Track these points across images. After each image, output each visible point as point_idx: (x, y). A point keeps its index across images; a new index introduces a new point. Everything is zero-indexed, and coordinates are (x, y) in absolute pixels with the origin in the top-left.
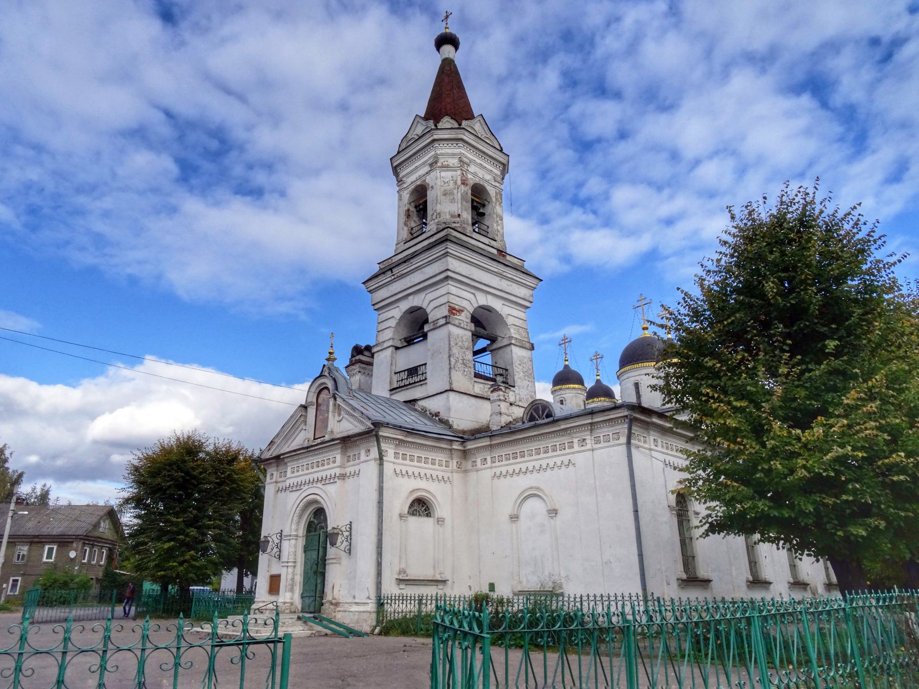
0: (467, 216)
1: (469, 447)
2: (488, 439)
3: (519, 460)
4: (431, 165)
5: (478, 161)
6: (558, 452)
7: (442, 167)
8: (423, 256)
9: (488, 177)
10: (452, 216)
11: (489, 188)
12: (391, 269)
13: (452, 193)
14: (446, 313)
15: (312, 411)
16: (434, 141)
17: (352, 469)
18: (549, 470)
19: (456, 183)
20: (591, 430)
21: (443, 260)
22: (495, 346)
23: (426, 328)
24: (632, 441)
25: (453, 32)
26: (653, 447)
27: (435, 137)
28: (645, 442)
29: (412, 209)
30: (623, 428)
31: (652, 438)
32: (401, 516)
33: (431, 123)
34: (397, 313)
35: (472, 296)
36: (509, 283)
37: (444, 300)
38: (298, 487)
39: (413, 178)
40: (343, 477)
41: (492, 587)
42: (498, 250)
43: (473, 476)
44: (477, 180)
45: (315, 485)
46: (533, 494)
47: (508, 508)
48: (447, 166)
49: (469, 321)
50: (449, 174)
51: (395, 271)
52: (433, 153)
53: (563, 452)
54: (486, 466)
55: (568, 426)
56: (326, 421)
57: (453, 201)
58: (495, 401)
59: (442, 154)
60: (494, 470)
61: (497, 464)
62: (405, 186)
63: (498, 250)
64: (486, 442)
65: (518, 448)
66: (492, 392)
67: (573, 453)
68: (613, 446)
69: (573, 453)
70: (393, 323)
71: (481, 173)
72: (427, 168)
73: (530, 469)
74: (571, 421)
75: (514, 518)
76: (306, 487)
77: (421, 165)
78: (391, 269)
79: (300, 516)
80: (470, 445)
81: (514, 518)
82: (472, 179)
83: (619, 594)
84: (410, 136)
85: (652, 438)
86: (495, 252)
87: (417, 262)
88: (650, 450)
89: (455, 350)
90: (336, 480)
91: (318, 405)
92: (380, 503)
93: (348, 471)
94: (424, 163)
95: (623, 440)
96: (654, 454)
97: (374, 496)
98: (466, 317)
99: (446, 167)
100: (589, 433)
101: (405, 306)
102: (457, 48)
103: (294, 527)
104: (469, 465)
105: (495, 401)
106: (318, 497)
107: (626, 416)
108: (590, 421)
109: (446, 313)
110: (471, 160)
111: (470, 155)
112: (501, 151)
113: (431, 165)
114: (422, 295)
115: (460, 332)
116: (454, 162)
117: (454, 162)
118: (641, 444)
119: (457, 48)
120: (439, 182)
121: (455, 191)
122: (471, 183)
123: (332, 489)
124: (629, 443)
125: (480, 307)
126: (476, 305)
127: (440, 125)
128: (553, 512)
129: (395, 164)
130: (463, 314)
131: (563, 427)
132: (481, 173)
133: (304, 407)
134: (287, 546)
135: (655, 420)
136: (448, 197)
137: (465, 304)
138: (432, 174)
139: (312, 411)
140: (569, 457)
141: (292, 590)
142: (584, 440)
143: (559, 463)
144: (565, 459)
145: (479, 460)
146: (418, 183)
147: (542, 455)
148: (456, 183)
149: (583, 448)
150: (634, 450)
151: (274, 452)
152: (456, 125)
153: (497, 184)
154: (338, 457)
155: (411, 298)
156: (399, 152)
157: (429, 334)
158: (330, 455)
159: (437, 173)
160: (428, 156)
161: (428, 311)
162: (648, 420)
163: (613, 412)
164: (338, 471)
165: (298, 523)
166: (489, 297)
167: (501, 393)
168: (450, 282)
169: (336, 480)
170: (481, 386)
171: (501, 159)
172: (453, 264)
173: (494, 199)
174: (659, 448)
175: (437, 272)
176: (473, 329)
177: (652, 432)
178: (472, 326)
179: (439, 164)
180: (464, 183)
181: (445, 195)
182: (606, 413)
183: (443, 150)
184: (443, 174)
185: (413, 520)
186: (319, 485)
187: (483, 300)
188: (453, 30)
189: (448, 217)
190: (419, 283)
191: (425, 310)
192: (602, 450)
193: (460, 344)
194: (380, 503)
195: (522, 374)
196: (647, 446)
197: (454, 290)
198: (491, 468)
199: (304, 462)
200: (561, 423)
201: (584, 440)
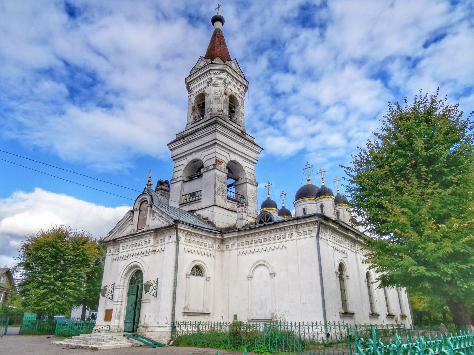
0: (226, 111)
1: (225, 237)
2: (237, 233)
3: (254, 245)
4: (208, 83)
5: (233, 83)
6: (277, 241)
7: (214, 84)
8: (202, 131)
9: (238, 92)
10: (219, 111)
11: (238, 98)
12: (183, 138)
13: (219, 99)
14: (214, 163)
15: (136, 213)
16: (210, 70)
17: (160, 248)
18: (271, 251)
19: (221, 93)
20: (296, 229)
21: (214, 134)
22: (237, 183)
23: (202, 171)
24: (320, 235)
25: (222, 15)
26: (328, 239)
27: (211, 68)
28: (325, 236)
29: (196, 106)
30: (315, 228)
31: (328, 234)
32: (187, 276)
33: (209, 61)
34: (185, 162)
35: (228, 155)
36: (247, 149)
37: (213, 155)
39: (197, 89)
40: (154, 252)
41: (235, 317)
42: (242, 131)
43: (226, 253)
44: (232, 93)
45: (136, 256)
46: (262, 264)
47: (247, 272)
48: (217, 84)
49: (225, 168)
50: (218, 88)
51: (186, 139)
52: (210, 76)
53: (280, 241)
54: (234, 248)
55: (283, 226)
56: (145, 219)
57: (219, 103)
58: (240, 212)
59: (214, 77)
60: (239, 250)
61: (241, 247)
62: (193, 93)
63: (242, 131)
64: (235, 234)
65: (253, 238)
66: (238, 207)
67: (286, 241)
68: (308, 238)
69: (286, 241)
70: (183, 168)
71: (234, 90)
72: (206, 85)
73: (260, 250)
74: (285, 223)
75: (250, 277)
76: (131, 257)
77: (202, 83)
78: (183, 138)
79: (127, 275)
80: (226, 236)
81: (250, 277)
82: (229, 93)
83: (314, 322)
84: (197, 67)
85: (328, 234)
86: (240, 132)
87: (198, 135)
88: (327, 240)
89: (218, 183)
90: (150, 253)
91: (140, 211)
92: (176, 267)
93: (157, 248)
94: (204, 82)
95: (315, 234)
96: (329, 243)
97: (173, 263)
98: (224, 166)
99: (217, 85)
100: (295, 230)
101: (190, 158)
102: (223, 23)
103: (122, 281)
104: (224, 247)
105: (240, 212)
106: (138, 264)
107: (317, 221)
108: (296, 223)
109: (214, 163)
110: (230, 82)
111: (229, 79)
112: (245, 79)
113: (208, 83)
114: (201, 153)
115: (221, 174)
116: (221, 82)
117: (221, 82)
118: (323, 237)
119: (223, 23)
120: (212, 92)
121: (221, 98)
122: (229, 94)
123: (146, 259)
124: (318, 236)
125: (231, 161)
126: (229, 160)
127: (214, 62)
128: (273, 275)
129: (188, 82)
130: (223, 164)
131: (280, 227)
132: (234, 90)
135: (331, 224)
137: (224, 158)
138: (209, 88)
139: (136, 213)
140: (283, 243)
142: (292, 234)
143: (277, 247)
144: (281, 245)
145: (230, 245)
146: (200, 92)
147: (267, 242)
148: (221, 93)
149: (291, 239)
150: (320, 240)
151: (112, 237)
152: (223, 63)
153: (242, 97)
154: (152, 240)
155: (194, 154)
156: (190, 75)
158: (147, 239)
160: (207, 78)
161: (203, 161)
162: (327, 224)
163: (310, 218)
164: (151, 248)
165: (125, 279)
166: (236, 156)
167: (243, 208)
168: (217, 146)
169: (150, 253)
170: (231, 204)
171: (244, 83)
172: (219, 136)
173: (240, 104)
174: (331, 240)
175: (210, 140)
176: (228, 172)
177: (328, 231)
178: (227, 171)
179: (213, 83)
180: (226, 94)
181: (215, 99)
182: (306, 219)
183: (215, 75)
184: (215, 88)
185: (194, 278)
186: (139, 256)
187: (233, 157)
188: (221, 14)
189: (216, 111)
191: (202, 161)
192: (302, 240)
193: (221, 180)
194: (176, 267)
195: (251, 199)
196: (325, 238)
197: (218, 151)
198: (238, 249)
199: (131, 243)
200: (280, 224)
201: (292, 234)
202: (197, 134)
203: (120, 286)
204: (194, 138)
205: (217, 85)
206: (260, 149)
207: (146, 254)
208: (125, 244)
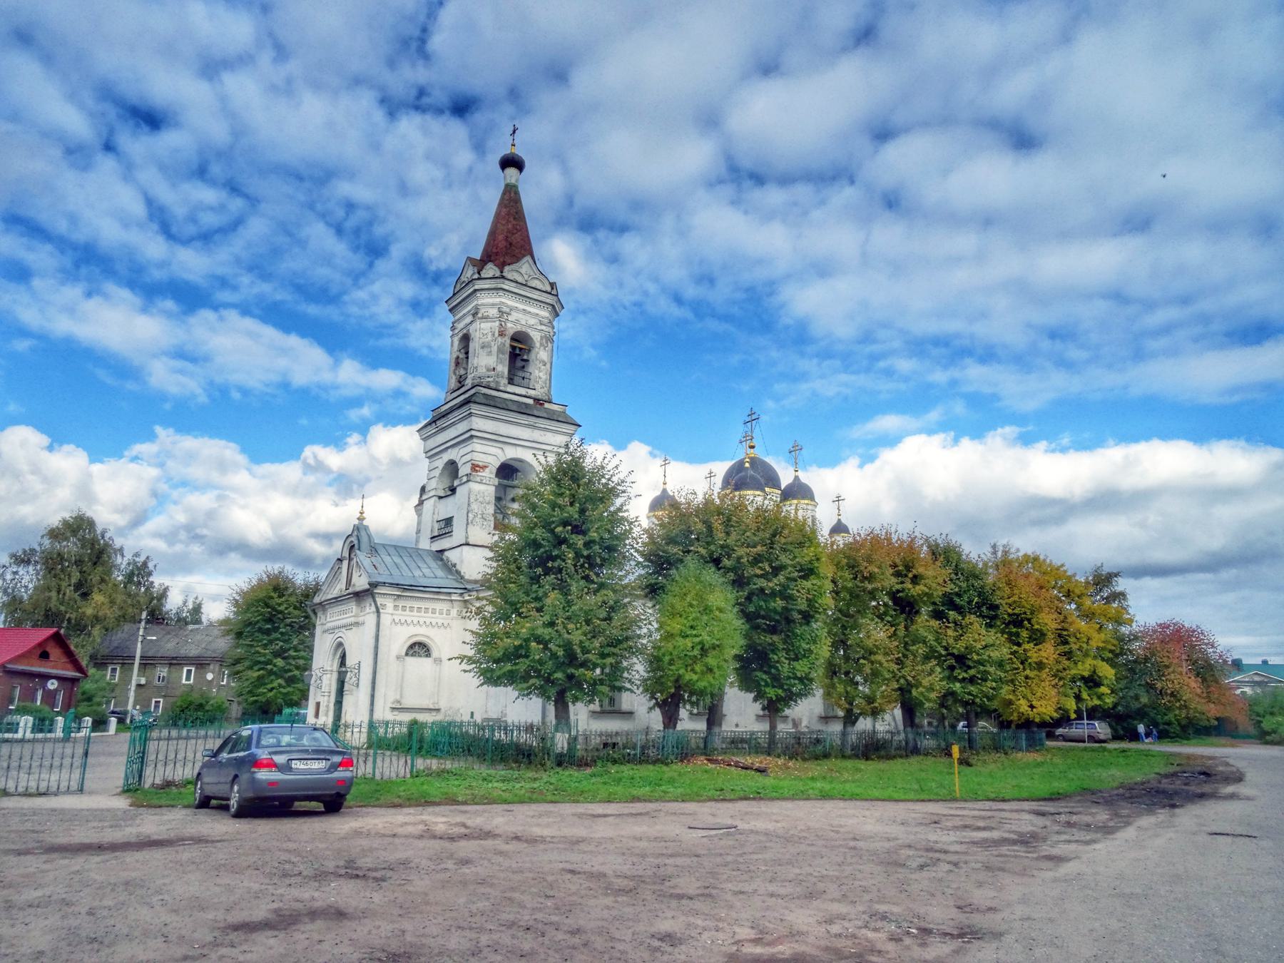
0: (503, 369)
5: (521, 306)
7: (482, 318)
8: (456, 413)
9: (532, 321)
14: (469, 471)
15: (345, 563)
16: (475, 291)
40: (357, 624)
42: (535, 399)
44: (519, 328)
50: (489, 325)
57: (490, 353)
63: (535, 399)
71: (523, 319)
79: (335, 654)
82: (511, 328)
89: (474, 506)
91: (350, 559)
92: (376, 648)
97: (372, 641)
99: (485, 318)
109: (469, 471)
111: (510, 302)
114: (456, 449)
117: (493, 312)
122: (510, 332)
133: (340, 560)
134: (326, 679)
136: (486, 350)
137: (489, 459)
139: (345, 563)
141: (327, 715)
152: (498, 274)
157: (458, 490)
159: (477, 325)
164: (353, 620)
166: (519, 449)
173: (538, 345)
180: (502, 334)
183: (485, 300)
184: (483, 325)
185: (410, 660)
187: (511, 453)
194: (376, 648)
202: (450, 416)
205: (485, 318)
206: (573, 427)
207: (348, 627)
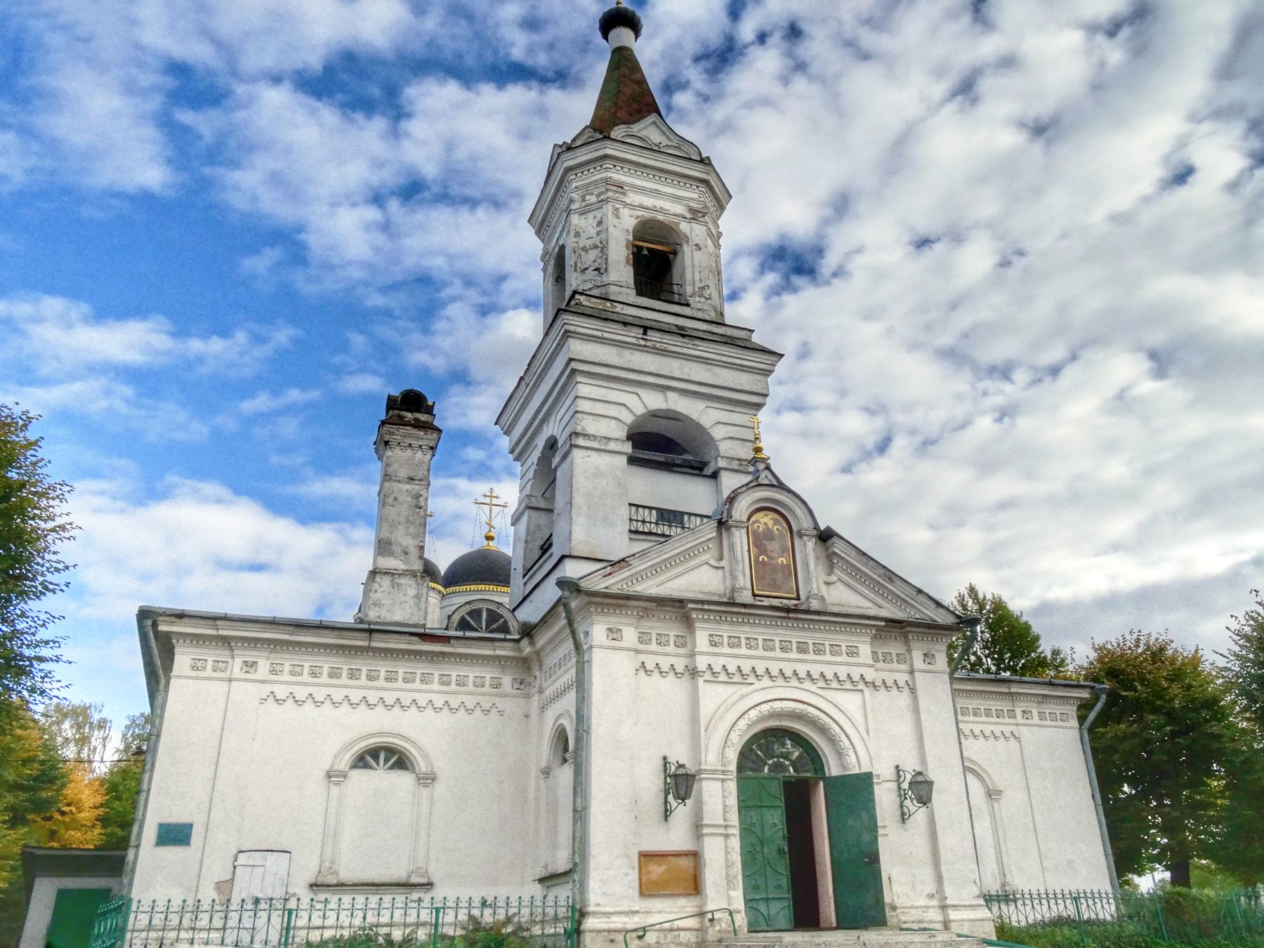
12: (646, 329)
38: (743, 677)
39: (648, 201)
78: (646, 329)
87: (703, 350)
90: (861, 686)
94: (677, 199)
101: (655, 401)
113: (692, 210)
123: (850, 702)
146: (660, 217)
155: (672, 395)
158: (844, 641)
175: (746, 388)
186: (807, 685)
190: (699, 384)
199: (760, 633)
203: (723, 772)
204: (685, 351)
208: (725, 631)
